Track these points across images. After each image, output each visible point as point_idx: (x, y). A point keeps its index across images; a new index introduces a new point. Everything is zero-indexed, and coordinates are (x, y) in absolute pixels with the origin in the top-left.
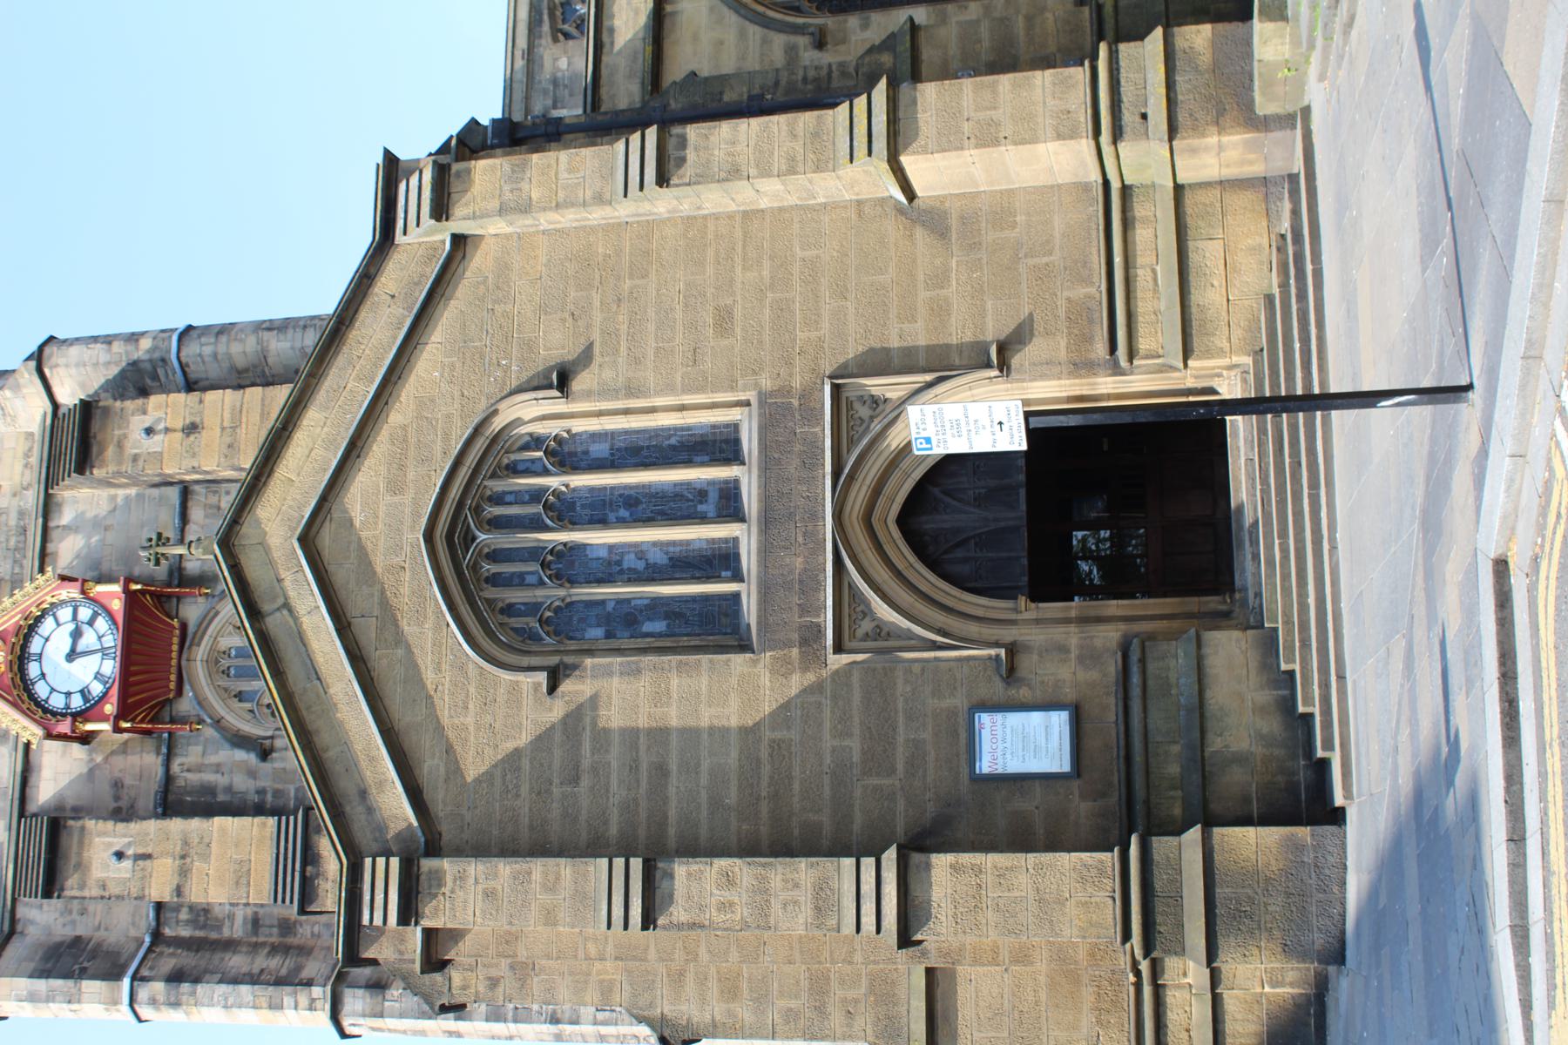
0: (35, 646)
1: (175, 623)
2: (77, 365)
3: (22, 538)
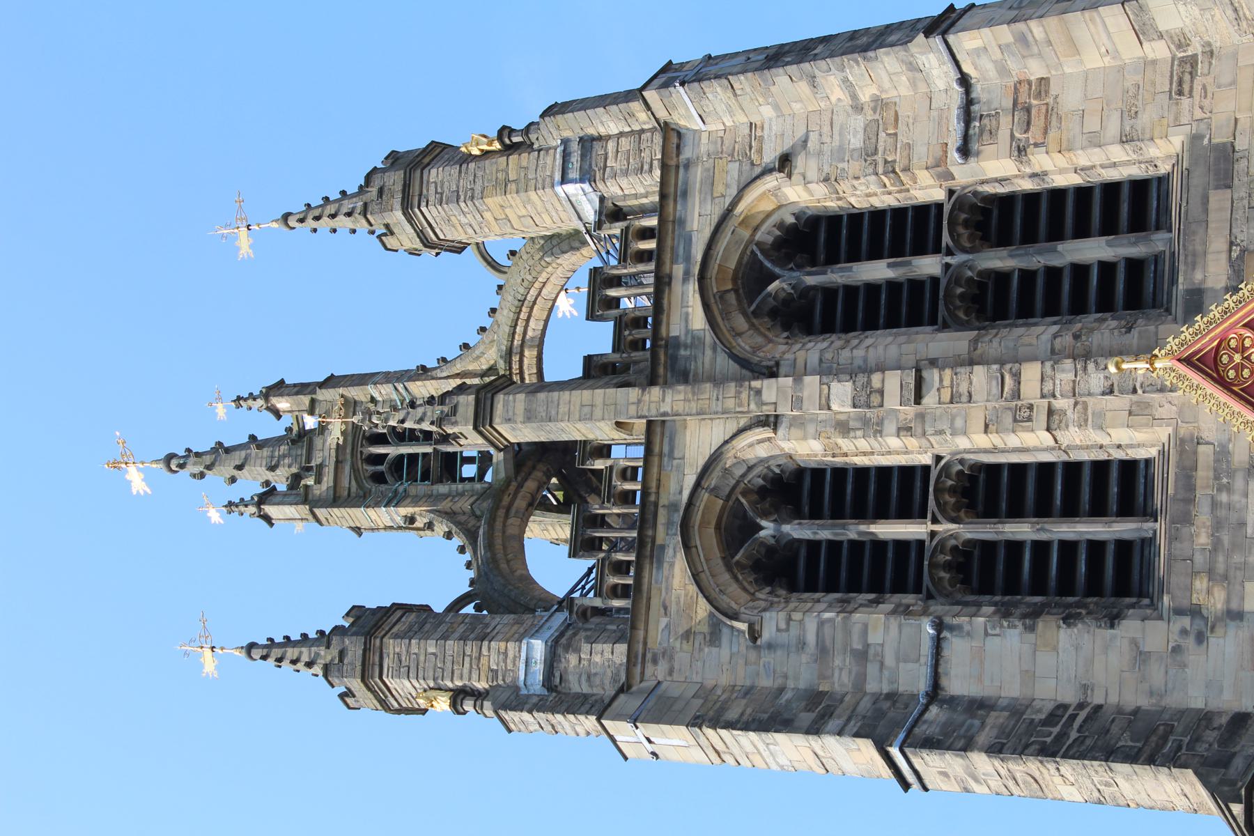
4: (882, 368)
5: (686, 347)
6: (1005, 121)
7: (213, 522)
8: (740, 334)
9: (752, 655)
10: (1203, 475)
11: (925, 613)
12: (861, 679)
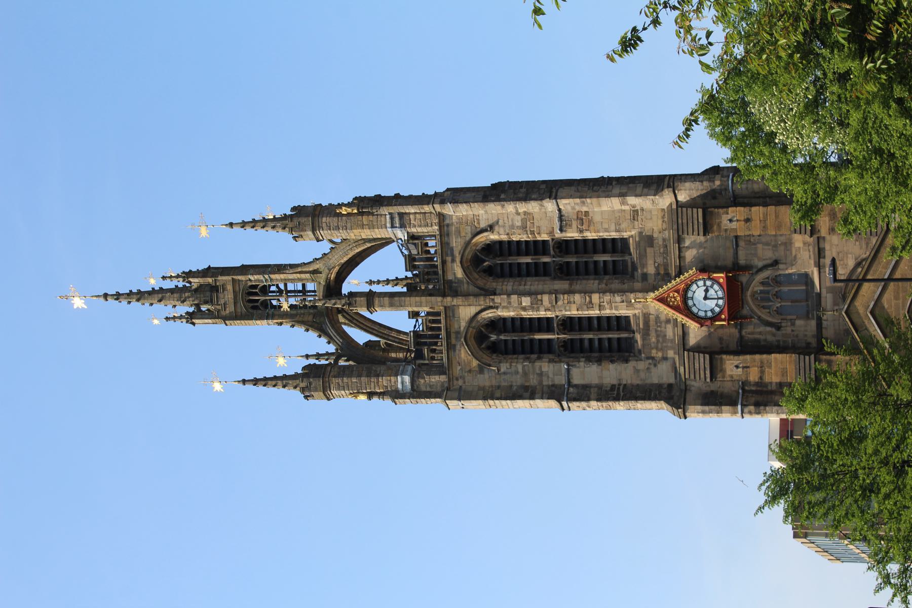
0: (690, 294)
1: (739, 284)
2: (690, 190)
3: (666, 249)
4: (542, 293)
5: (455, 283)
6: (574, 224)
7: (75, 307)
8: (477, 280)
9: (498, 376)
10: (652, 323)
11: (560, 361)
12: (541, 382)
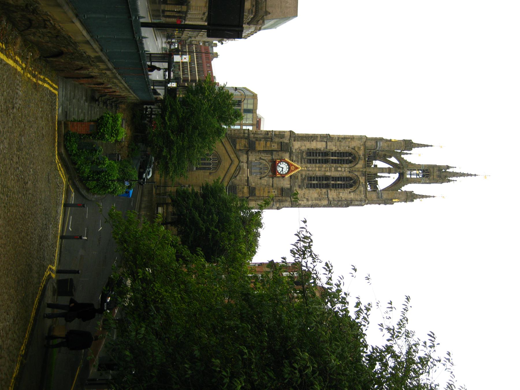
0: (288, 169)
10: (300, 161)
11: (329, 149)
12: (336, 143)
